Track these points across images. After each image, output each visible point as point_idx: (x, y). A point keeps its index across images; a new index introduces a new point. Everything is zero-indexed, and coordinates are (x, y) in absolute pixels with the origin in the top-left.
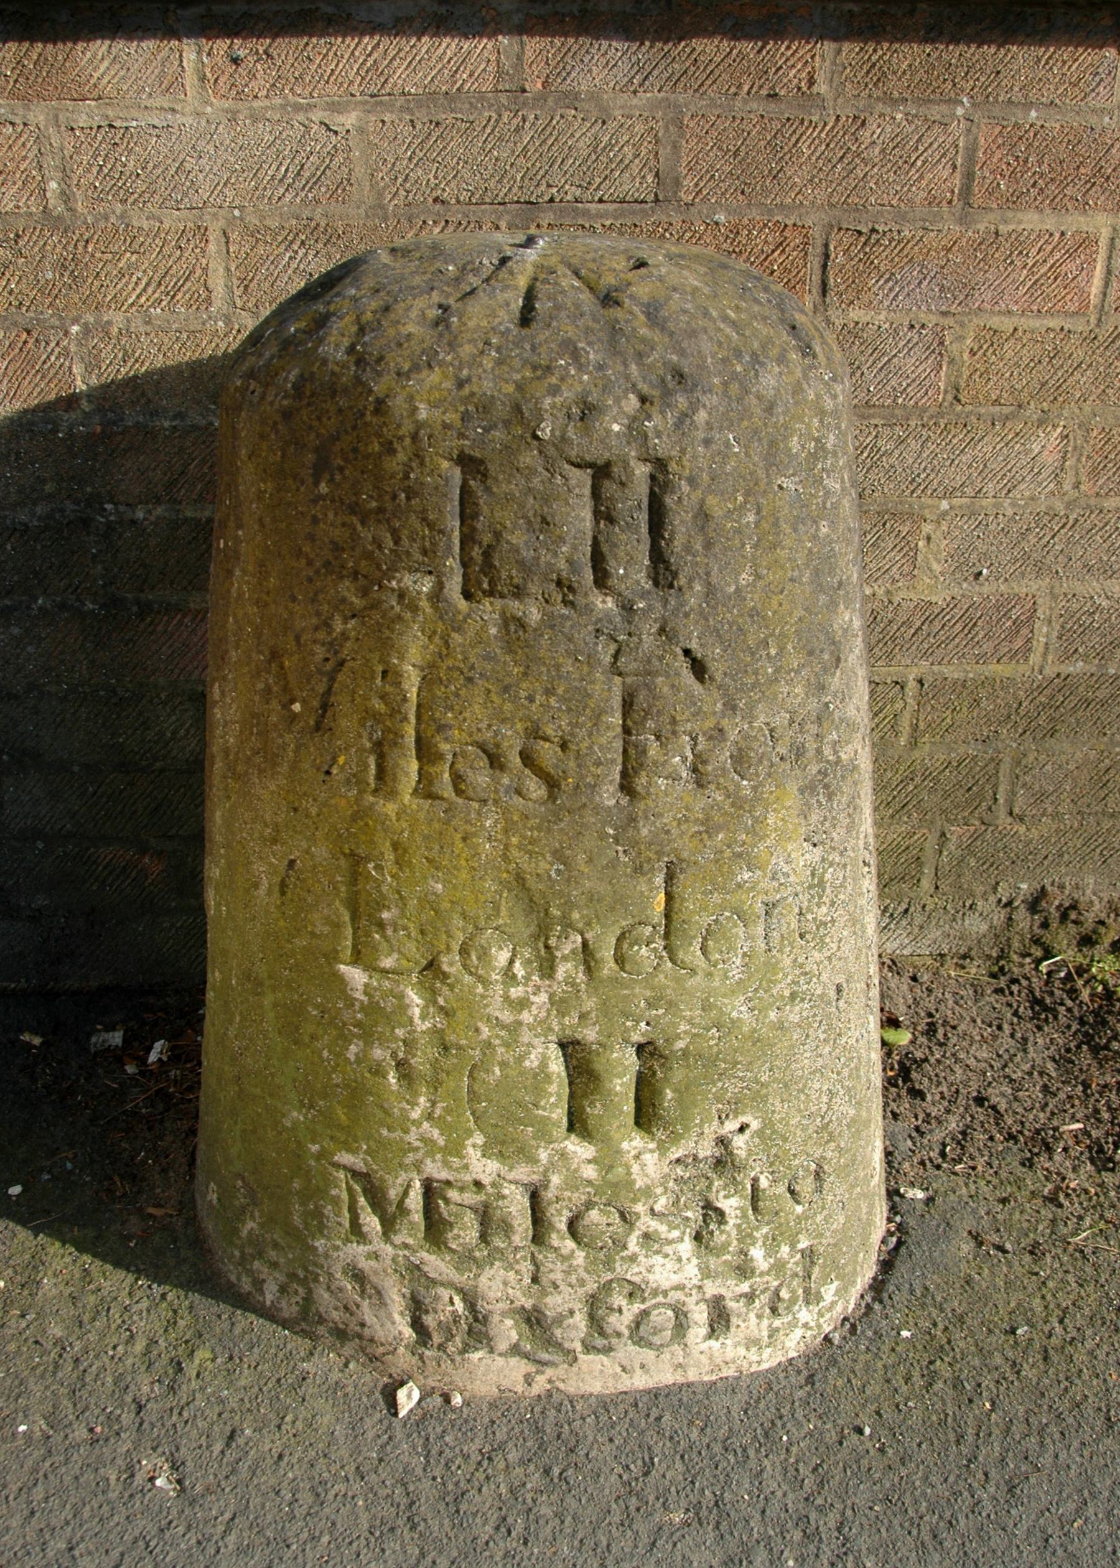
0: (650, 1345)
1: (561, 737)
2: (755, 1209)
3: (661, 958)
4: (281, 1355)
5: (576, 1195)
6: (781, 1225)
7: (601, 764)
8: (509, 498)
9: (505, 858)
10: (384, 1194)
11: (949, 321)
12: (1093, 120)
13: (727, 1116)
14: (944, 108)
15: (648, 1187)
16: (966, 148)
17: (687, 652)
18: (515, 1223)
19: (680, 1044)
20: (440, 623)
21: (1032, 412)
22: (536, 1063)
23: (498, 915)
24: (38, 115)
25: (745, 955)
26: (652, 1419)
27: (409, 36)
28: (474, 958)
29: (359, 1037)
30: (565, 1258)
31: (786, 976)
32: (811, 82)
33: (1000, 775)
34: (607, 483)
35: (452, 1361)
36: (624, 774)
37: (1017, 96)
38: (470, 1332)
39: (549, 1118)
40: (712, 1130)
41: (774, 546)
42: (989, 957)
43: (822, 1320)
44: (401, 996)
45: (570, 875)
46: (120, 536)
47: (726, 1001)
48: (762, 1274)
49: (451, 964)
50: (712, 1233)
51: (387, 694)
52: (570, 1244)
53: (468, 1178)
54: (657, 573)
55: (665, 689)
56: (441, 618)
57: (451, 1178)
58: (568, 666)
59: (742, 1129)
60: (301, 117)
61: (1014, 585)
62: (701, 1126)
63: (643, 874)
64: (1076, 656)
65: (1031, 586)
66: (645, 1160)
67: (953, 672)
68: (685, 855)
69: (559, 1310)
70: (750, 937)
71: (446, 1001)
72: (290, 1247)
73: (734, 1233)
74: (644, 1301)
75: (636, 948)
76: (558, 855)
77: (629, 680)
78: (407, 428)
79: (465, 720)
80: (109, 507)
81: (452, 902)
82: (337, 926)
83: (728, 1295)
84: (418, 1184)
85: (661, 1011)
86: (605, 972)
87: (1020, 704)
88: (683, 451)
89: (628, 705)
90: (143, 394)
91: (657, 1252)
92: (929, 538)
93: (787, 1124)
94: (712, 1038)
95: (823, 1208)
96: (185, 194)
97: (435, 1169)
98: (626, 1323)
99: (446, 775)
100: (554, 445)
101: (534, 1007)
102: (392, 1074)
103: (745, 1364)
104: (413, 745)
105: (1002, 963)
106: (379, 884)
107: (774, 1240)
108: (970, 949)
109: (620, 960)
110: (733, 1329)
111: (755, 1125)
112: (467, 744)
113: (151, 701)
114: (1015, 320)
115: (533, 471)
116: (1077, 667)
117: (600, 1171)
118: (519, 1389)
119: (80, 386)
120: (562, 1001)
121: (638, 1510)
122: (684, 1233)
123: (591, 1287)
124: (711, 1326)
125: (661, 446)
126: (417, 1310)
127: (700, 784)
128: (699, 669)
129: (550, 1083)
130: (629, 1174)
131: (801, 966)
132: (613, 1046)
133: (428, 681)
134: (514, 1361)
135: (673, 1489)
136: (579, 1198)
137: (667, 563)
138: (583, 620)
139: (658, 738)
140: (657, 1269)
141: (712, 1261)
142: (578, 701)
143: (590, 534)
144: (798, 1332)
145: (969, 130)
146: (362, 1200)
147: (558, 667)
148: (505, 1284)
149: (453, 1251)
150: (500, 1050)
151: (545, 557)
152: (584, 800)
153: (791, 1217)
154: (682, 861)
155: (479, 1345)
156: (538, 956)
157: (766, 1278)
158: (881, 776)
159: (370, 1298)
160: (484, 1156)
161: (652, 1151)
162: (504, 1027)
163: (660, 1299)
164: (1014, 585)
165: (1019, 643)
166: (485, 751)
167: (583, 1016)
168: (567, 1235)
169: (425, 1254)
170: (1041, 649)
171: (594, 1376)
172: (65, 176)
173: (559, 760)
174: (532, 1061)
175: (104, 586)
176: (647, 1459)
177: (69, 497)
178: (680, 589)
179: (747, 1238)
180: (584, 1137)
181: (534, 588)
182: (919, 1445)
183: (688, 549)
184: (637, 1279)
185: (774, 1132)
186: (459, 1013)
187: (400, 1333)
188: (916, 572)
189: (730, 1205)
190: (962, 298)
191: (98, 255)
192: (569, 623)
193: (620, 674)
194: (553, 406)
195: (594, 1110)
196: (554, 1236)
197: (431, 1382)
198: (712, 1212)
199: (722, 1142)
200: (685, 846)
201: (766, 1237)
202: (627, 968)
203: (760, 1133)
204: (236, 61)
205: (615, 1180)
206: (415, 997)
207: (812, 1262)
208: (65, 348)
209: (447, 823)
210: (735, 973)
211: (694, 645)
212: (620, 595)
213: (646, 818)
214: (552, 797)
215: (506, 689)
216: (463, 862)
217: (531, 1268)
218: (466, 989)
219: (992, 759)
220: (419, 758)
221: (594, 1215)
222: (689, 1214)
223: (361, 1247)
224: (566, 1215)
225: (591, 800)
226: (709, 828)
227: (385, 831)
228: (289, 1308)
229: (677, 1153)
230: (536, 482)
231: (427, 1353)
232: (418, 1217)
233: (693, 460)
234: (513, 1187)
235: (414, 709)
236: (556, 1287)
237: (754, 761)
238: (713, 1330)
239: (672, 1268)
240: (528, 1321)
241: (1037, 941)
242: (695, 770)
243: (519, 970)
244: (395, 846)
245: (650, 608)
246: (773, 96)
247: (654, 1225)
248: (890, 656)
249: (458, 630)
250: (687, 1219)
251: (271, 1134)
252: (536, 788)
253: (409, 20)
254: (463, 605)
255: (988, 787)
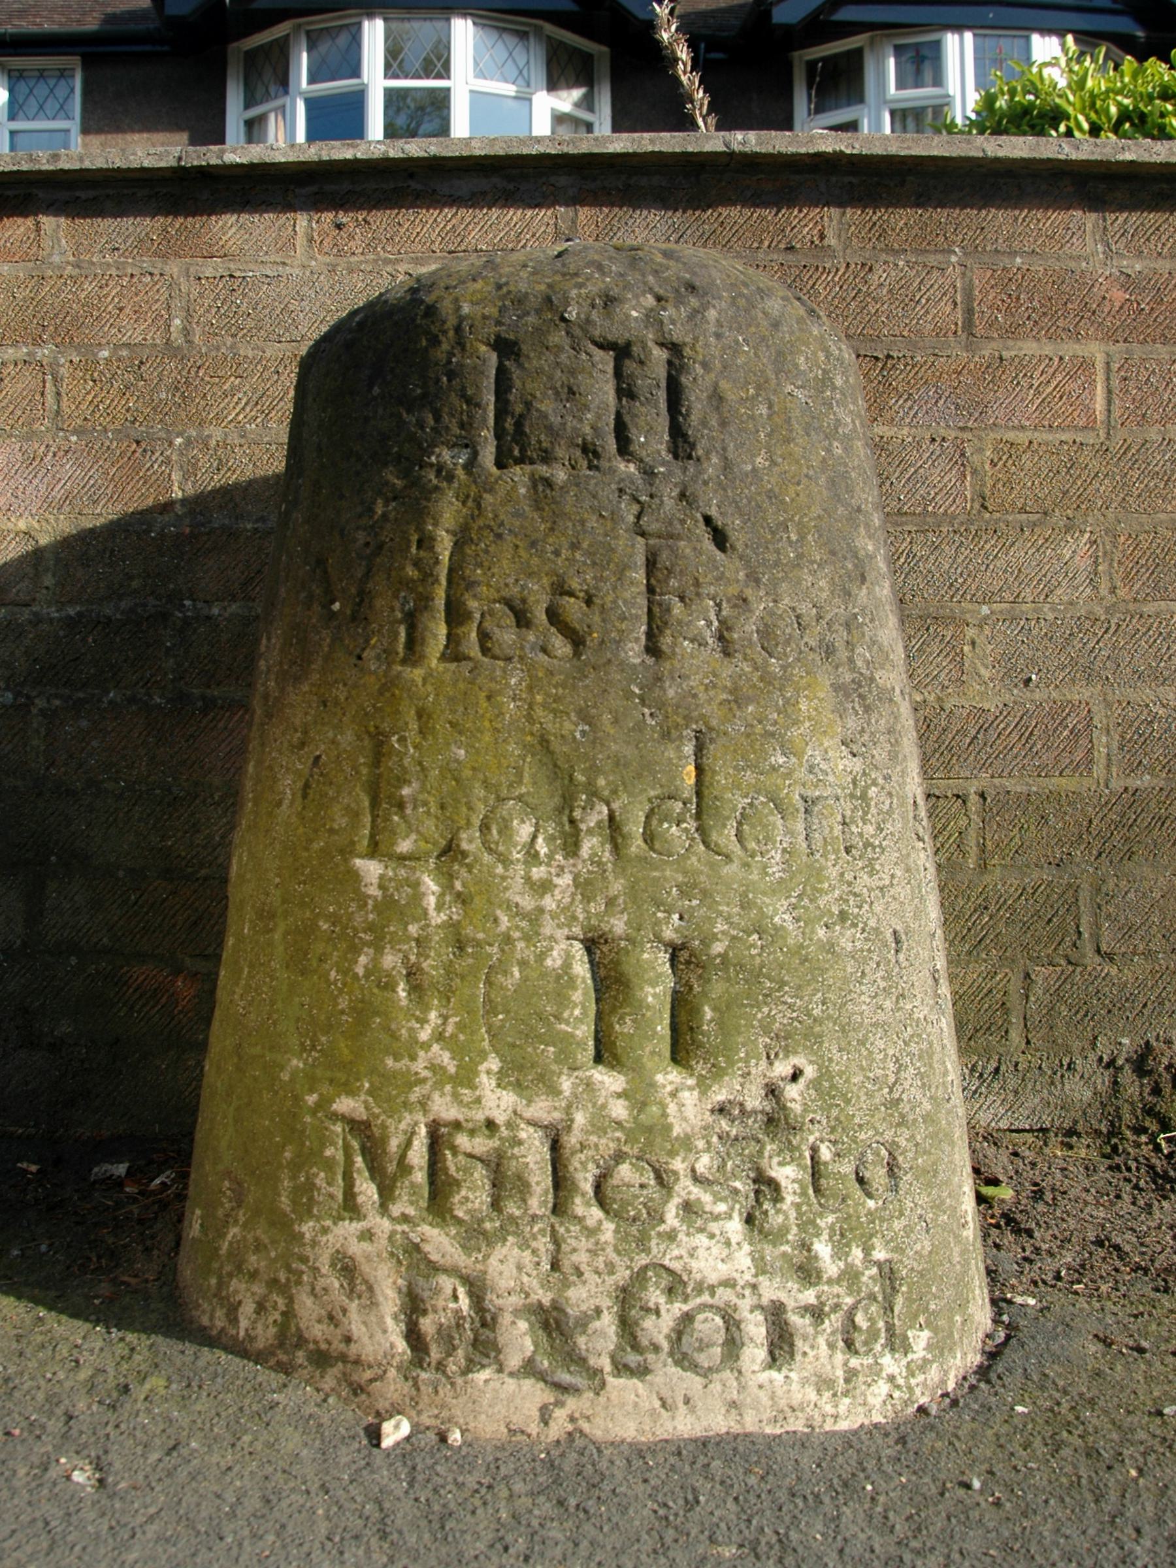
0: (694, 1367)
1: (586, 592)
2: (817, 1190)
3: (693, 839)
4: (248, 1386)
5: (603, 1141)
6: (850, 1216)
7: (625, 618)
8: (539, 372)
9: (530, 718)
10: (384, 1140)
11: (967, 435)
12: (1072, 265)
13: (776, 1055)
14: (940, 257)
15: (688, 1137)
16: (964, 289)
17: (708, 520)
18: (533, 1180)
19: (718, 948)
20: (473, 487)
21: (1058, 518)
22: (559, 962)
23: (520, 782)
24: (174, 268)
25: (784, 850)
26: (698, 1466)
27: (482, 208)
28: (494, 832)
29: (369, 944)
30: (592, 1232)
31: (833, 888)
32: (822, 237)
33: (1080, 903)
34: (627, 362)
35: (453, 1384)
36: (650, 635)
37: (1001, 246)
38: (475, 1343)
39: (572, 1035)
40: (759, 1068)
41: (788, 441)
42: (1098, 1132)
43: (913, 1381)
44: (417, 884)
45: (595, 739)
46: (195, 630)
47: (767, 901)
48: (830, 1282)
49: (470, 841)
50: (766, 1213)
51: (420, 559)
52: (596, 1213)
53: (480, 1116)
54: (676, 447)
55: (688, 551)
56: (475, 482)
57: (461, 1117)
58: (593, 522)
59: (795, 1077)
60: (389, 269)
61: (1066, 691)
62: (747, 1061)
63: (672, 741)
64: (1141, 768)
65: (1081, 693)
66: (684, 1101)
67: (1016, 786)
68: (714, 723)
69: (584, 1308)
70: (790, 832)
71: (464, 885)
72: (273, 1242)
73: (793, 1214)
74: (685, 1301)
75: (666, 825)
76: (584, 716)
77: (651, 542)
78: (452, 322)
79: (493, 575)
80: (187, 603)
81: (474, 769)
82: (356, 815)
83: (790, 1304)
84: (423, 1131)
85: (695, 902)
86: (633, 849)
87: (1090, 821)
88: (696, 339)
89: (651, 564)
90: (231, 500)
91: (701, 1230)
92: (973, 643)
93: (847, 1081)
94: (753, 946)
95: (902, 1214)
96: (287, 329)
97: (444, 1108)
98: (666, 1331)
99: (474, 635)
100: (580, 327)
101: (557, 892)
102: (402, 985)
103: (818, 1419)
104: (442, 607)
105: (1114, 1141)
106: (401, 755)
107: (842, 1235)
108: (1075, 1122)
109: (649, 838)
110: (798, 1357)
111: (810, 1071)
112: (495, 601)
113: (204, 801)
114: (1029, 434)
115: (560, 348)
116: (1144, 781)
117: (631, 1108)
118: (534, 1429)
119: (177, 494)
120: (588, 882)
121: (676, 1541)
122: (732, 1209)
123: (622, 1275)
124: (771, 1353)
125: (678, 333)
126: (414, 1306)
127: (727, 653)
128: (720, 539)
129: (575, 989)
130: (665, 1115)
131: (850, 884)
132: (642, 944)
133: (458, 546)
134: (528, 1384)
135: (723, 1525)
136: (607, 1145)
137: (685, 436)
138: (607, 479)
139: (682, 599)
140: (701, 1252)
141: (769, 1252)
142: (602, 557)
143: (613, 410)
144: (883, 1388)
145: (964, 274)
146: (359, 1160)
147: (583, 522)
148: (520, 1268)
149: (459, 1221)
150: (520, 945)
151: (571, 422)
152: (609, 655)
153: (863, 1212)
154: (711, 729)
155: (485, 1361)
156: (562, 832)
157: (836, 1289)
158: (952, 904)
159: (359, 1297)
160: (499, 1086)
161: (691, 1089)
162: (524, 916)
163: (706, 1298)
164: (1066, 691)
165: (1079, 755)
166: (512, 608)
167: (611, 902)
168: (593, 1201)
169: (426, 1229)
170: (1103, 761)
171: (627, 1412)
172: (189, 314)
173: (584, 614)
174: (554, 961)
175: (172, 681)
176: (690, 1497)
177: (152, 593)
178: (698, 460)
179: (807, 1225)
180: (613, 1068)
181: (560, 452)
182: (1046, 1502)
183: (704, 423)
184: (676, 1266)
185: (832, 1086)
186: (477, 900)
187: (392, 1346)
188: (964, 678)
189: (786, 1174)
190: (977, 415)
191: (207, 379)
192: (593, 482)
193: (643, 534)
194: (579, 295)
195: (624, 1028)
196: (578, 1200)
197: (426, 1420)
198: (765, 1185)
199: (772, 1091)
200: (711, 710)
201: (832, 1228)
202: (657, 846)
203: (815, 1084)
204: (339, 227)
205: (648, 1122)
206: (431, 883)
207: (893, 1288)
208: (168, 457)
209: (472, 682)
210: (776, 871)
211: (713, 512)
212: (641, 461)
213: (673, 678)
214: (577, 654)
215: (533, 544)
216: (487, 724)
217: (551, 1247)
218: (485, 869)
219: (1070, 885)
220: (448, 622)
221: (625, 1171)
222: (738, 1184)
223: (354, 1224)
224: (592, 1172)
225: (616, 656)
226: (737, 699)
227: (411, 698)
228: (265, 1335)
229: (720, 1095)
230: (563, 357)
231: (424, 1375)
232: (420, 1177)
233: (705, 347)
234: (531, 1129)
235: (445, 571)
236: (579, 1273)
237: (781, 639)
238: (774, 1359)
239: (718, 1254)
240: (546, 1326)
241: (1150, 1111)
242: (721, 638)
243: (542, 847)
244: (420, 714)
245: (671, 472)
246: (790, 249)
247: (696, 1192)
248: (948, 766)
249: (491, 491)
250: (736, 1191)
251: (266, 1096)
252: (561, 646)
253: (484, 193)
254: (494, 470)
255: (1069, 918)
